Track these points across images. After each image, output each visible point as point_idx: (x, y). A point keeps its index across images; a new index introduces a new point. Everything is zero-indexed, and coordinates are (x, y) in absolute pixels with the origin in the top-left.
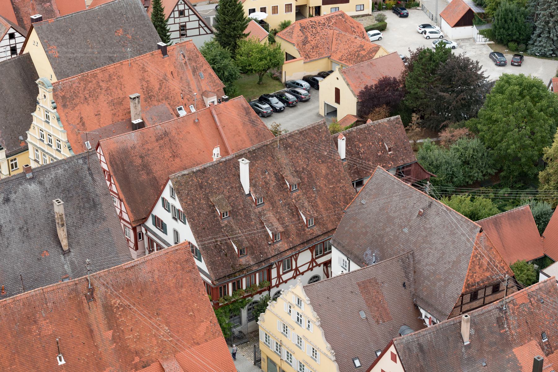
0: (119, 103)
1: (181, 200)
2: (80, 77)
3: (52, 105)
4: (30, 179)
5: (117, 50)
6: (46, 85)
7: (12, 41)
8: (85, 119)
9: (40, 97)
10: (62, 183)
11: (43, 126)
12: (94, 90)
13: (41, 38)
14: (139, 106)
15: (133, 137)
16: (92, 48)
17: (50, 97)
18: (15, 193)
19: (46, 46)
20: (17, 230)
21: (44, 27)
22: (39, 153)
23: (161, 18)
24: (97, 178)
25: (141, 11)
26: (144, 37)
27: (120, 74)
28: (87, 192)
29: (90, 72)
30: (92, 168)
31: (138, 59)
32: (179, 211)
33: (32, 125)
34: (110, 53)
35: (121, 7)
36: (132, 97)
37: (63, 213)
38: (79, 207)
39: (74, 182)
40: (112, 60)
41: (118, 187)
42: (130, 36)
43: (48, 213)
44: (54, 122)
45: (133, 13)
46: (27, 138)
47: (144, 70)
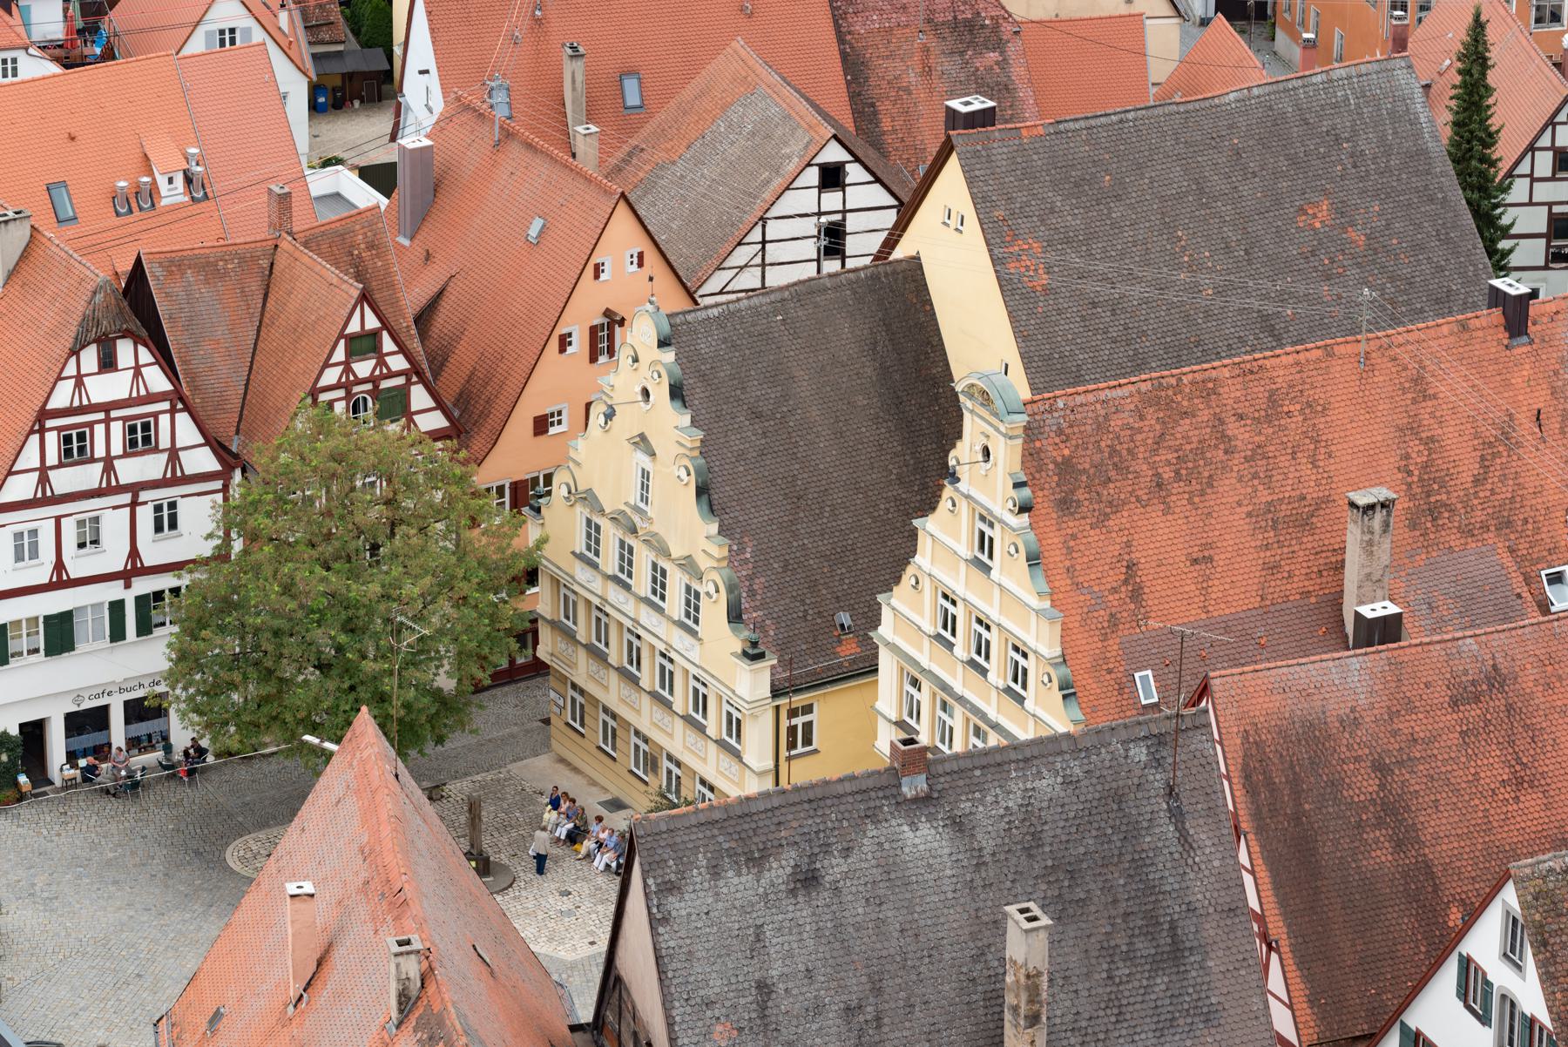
0: (1298, 520)
1: (1548, 979)
2: (1144, 387)
3: (1013, 493)
4: (915, 800)
5: (1301, 289)
6: (998, 403)
7: (832, 200)
8: (1145, 574)
9: (963, 453)
10: (1047, 838)
12: (1200, 452)
13: (980, 201)
15: (1351, 678)
16: (1194, 267)
17: (1008, 455)
20: (832, 1018)
22: (924, 697)
23: (1483, 175)
24: (1201, 834)
25: (1418, 135)
26: (1418, 248)
27: (1319, 394)
28: (1151, 889)
29: (1189, 373)
30: (1184, 790)
31: (1401, 339)
32: (1532, 1022)
33: (910, 570)
34: (1265, 297)
35: (1335, 106)
36: (1362, 499)
37: (1044, 966)
38: (1109, 952)
39: (1102, 838)
40: (1272, 332)
41: (1267, 885)
42: (1357, 236)
43: (975, 959)
44: (1010, 571)
45: (1382, 139)
46: (875, 621)
47: (1420, 388)
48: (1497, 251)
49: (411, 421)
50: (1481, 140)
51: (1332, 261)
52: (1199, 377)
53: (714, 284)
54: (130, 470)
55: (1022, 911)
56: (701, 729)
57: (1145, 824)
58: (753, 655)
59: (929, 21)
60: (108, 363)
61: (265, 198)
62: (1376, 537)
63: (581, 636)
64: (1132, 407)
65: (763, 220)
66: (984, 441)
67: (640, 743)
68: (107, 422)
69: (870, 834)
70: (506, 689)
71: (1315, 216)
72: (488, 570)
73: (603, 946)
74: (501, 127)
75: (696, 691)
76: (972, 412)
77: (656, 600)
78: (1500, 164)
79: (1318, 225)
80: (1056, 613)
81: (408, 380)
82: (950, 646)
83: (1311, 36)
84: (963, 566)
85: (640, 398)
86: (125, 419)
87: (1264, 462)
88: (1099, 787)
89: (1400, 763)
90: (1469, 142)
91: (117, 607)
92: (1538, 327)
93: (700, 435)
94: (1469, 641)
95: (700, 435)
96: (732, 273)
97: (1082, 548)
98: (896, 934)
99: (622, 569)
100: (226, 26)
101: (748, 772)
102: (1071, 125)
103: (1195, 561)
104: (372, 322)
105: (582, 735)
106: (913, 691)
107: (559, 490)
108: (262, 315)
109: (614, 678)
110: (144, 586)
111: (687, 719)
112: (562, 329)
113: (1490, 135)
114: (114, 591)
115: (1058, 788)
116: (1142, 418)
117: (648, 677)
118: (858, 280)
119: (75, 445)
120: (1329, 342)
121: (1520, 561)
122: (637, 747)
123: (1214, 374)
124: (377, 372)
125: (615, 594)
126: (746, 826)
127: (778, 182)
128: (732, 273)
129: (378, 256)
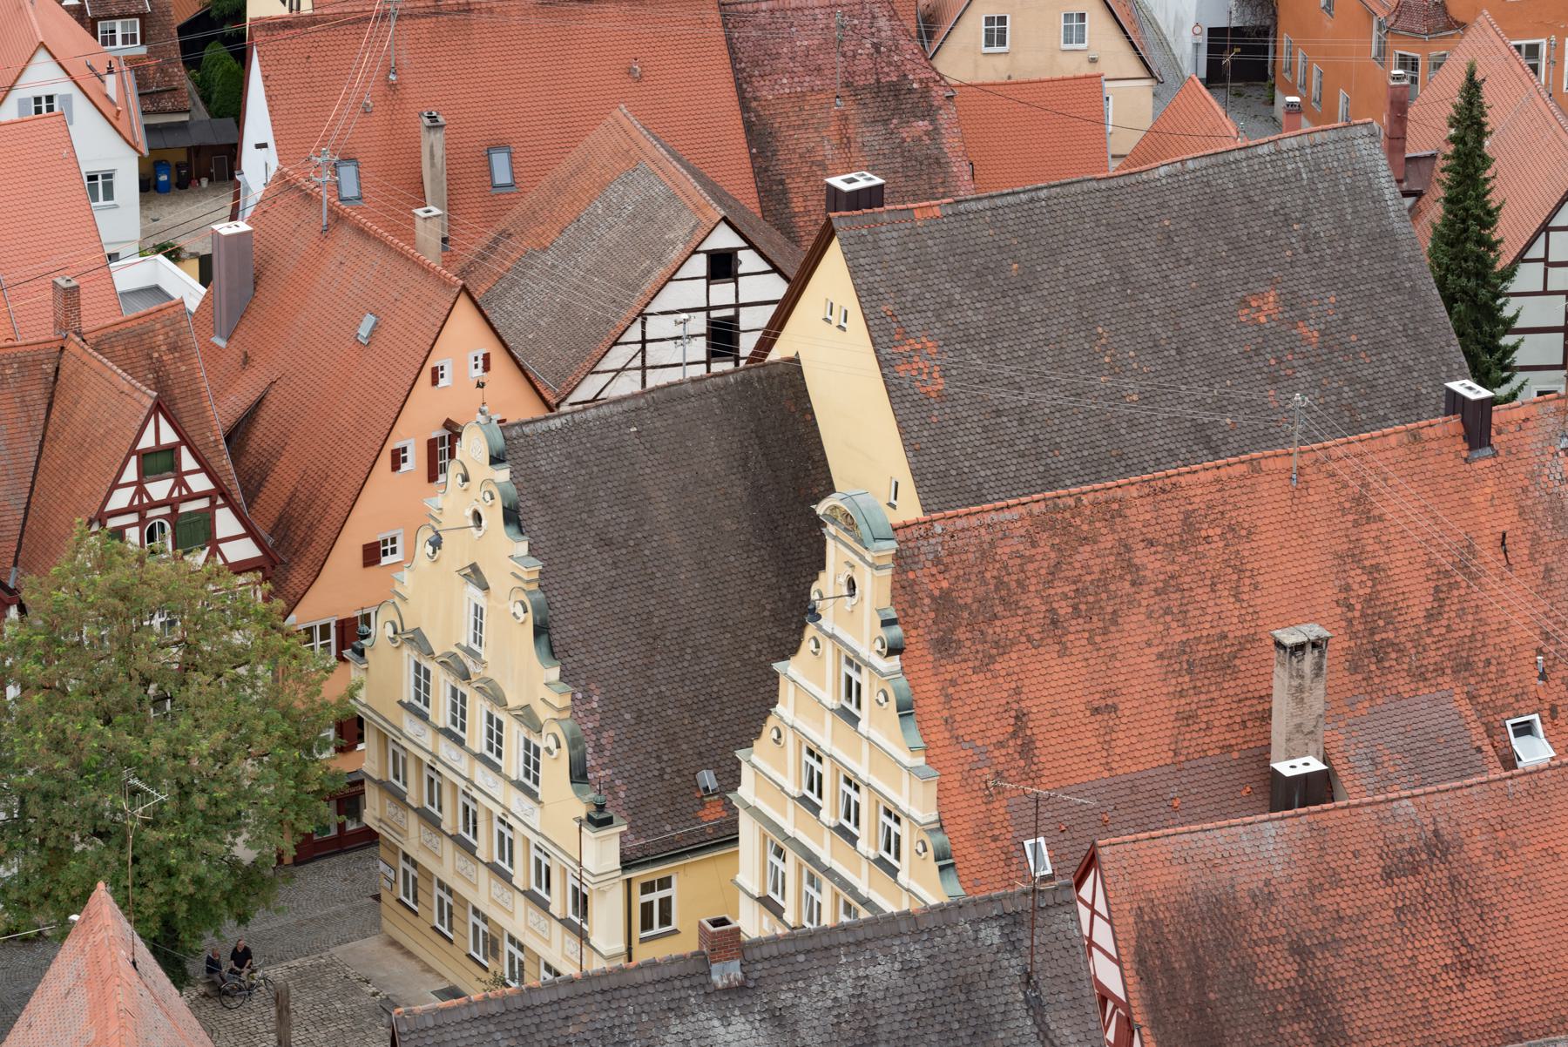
0: (1219, 666)
3: (882, 633)
4: (728, 990)
6: (863, 528)
7: (722, 293)
8: (1038, 726)
9: (827, 584)
11: (825, 734)
12: (1103, 583)
13: (866, 294)
14: (1320, 690)
15: (1266, 845)
16: (1117, 370)
17: (876, 589)
19: (887, 337)
21: (889, 237)
22: (789, 867)
23: (1480, 259)
25: (1383, 213)
26: (1380, 345)
29: (1090, 493)
31: (1339, 452)
33: (772, 722)
34: (1200, 403)
35: (1285, 181)
36: (1290, 639)
40: (1208, 442)
42: (1309, 332)
44: (879, 722)
45: (1341, 218)
46: (737, 781)
47: (1362, 509)
48: (1498, 347)
49: (215, 550)
50: (1477, 218)
51: (1280, 361)
52: (1101, 497)
53: (586, 391)
56: (544, 906)
57: (998, 1018)
58: (598, 820)
59: (847, 85)
61: (49, 294)
62: (1307, 682)
63: (412, 799)
64: (1023, 532)
65: (643, 316)
66: (849, 572)
70: (335, 860)
71: (1259, 309)
72: (295, 721)
74: (330, 210)
75: (538, 862)
76: (835, 538)
77: (493, 756)
78: (1501, 247)
79: (1263, 319)
80: (931, 771)
81: (213, 503)
82: (816, 809)
83: (1296, 99)
84: (828, 716)
85: (471, 523)
87: (1178, 595)
88: (944, 975)
89: (1323, 945)
90: (1464, 221)
92: (1504, 437)
93: (538, 565)
94: (1405, 802)
95: (538, 565)
96: (607, 377)
97: (963, 695)
99: (454, 722)
101: (595, 955)
102: (973, 206)
103: (1096, 711)
104: (169, 436)
105: (416, 914)
106: (777, 862)
107: (381, 630)
108: (45, 428)
109: (448, 847)
111: (529, 895)
112: (395, 443)
113: (1489, 213)
115: (895, 975)
116: (1034, 544)
117: (486, 847)
118: (726, 386)
120: (1256, 454)
121: (1481, 708)
122: (476, 927)
123: (1119, 493)
124: (176, 494)
125: (446, 750)
126: (528, 1021)
127: (660, 272)
128: (607, 377)
129: (181, 359)
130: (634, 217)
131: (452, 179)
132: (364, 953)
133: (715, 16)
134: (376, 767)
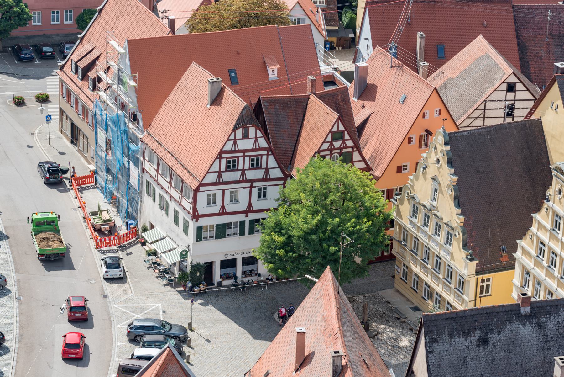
4: (525, 316)
7: (511, 96)
9: (551, 192)
18: (499, 333)
54: (250, 175)
55: (561, 359)
59: (550, 34)
60: (246, 136)
67: (427, 287)
68: (244, 157)
69: (508, 327)
70: (380, 264)
73: (408, 360)
76: (556, 176)
81: (353, 149)
85: (436, 162)
86: (250, 156)
91: (242, 223)
95: (456, 178)
96: (473, 119)
98: (514, 364)
100: (297, 18)
104: (341, 128)
110: (253, 216)
114: (242, 217)
119: (232, 164)
122: (425, 289)
124: (342, 146)
128: (473, 119)
129: (345, 104)
130: (484, 70)
131: (426, 54)
132: (388, 294)
133: (510, 9)
134: (398, 236)
